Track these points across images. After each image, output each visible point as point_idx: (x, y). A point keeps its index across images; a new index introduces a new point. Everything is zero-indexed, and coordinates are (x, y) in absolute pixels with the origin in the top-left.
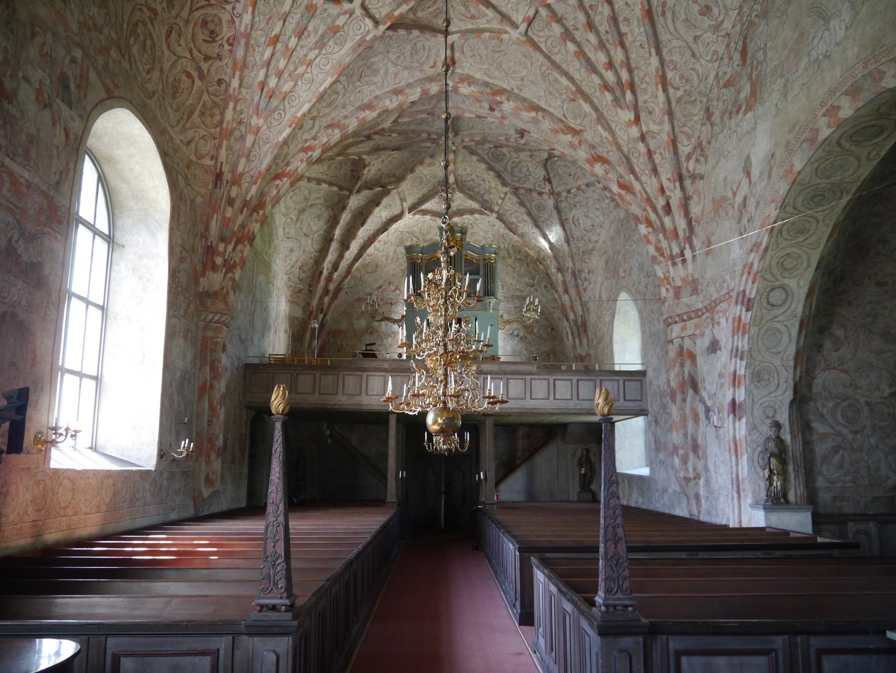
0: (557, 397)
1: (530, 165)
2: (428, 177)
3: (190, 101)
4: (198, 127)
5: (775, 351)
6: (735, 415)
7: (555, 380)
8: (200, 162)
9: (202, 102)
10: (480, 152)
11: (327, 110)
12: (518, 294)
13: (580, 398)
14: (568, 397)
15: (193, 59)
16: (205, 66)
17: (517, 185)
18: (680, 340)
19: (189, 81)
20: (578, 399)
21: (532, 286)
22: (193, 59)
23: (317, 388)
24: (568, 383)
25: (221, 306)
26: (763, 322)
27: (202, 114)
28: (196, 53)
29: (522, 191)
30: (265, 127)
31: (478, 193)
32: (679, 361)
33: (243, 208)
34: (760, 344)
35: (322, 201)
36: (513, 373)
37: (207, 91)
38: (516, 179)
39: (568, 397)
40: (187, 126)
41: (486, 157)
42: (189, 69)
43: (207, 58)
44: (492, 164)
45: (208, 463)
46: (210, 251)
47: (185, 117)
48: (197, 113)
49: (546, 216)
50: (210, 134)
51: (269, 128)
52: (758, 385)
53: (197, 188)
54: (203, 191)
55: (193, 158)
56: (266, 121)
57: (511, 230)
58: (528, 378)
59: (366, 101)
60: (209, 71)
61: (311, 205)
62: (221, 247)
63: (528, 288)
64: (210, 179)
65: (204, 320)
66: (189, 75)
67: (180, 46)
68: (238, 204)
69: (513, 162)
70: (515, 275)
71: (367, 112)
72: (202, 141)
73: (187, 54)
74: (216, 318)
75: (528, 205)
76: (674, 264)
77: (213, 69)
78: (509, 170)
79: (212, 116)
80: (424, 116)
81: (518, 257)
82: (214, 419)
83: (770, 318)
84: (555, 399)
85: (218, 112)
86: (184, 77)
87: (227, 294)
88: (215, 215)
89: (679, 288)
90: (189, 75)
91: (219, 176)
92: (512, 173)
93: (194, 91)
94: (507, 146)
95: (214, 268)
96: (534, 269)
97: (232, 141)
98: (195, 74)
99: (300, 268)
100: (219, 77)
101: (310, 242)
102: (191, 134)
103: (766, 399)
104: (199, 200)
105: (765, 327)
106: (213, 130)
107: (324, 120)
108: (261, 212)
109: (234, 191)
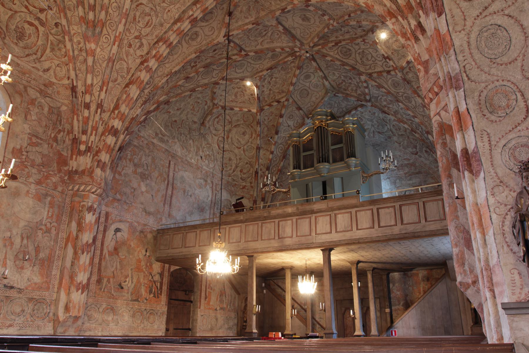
0: (381, 225)
1: (371, 50)
2: (311, 88)
3: (40, 43)
4: (52, 59)
5: (505, 59)
6: (471, 172)
7: (378, 209)
8: (60, 82)
9: (49, 42)
10: (331, 54)
11: (148, 30)
12: (406, 162)
13: (405, 222)
14: (393, 223)
15: (31, 13)
16: (42, 16)
17: (370, 71)
18: (437, 117)
19: (32, 29)
20: (402, 223)
21: (416, 154)
22: (31, 13)
23: (197, 242)
24: (392, 210)
25: (86, 179)
26: (469, 23)
27: (53, 50)
28: (31, 8)
29: (375, 75)
30: (98, 50)
31: (352, 90)
32: (440, 141)
33: (97, 109)
34: (477, 56)
35: (242, 122)
36: (339, 208)
37: (50, 33)
38: (368, 67)
39: (393, 223)
40: (43, 58)
41: (337, 56)
42: (28, 19)
43: (42, 10)
44: (344, 60)
45: (68, 294)
46: (75, 141)
47: (39, 54)
48: (48, 50)
49: (402, 90)
50: (62, 62)
51: (102, 50)
52: (493, 118)
53: (61, 100)
54: (66, 102)
55: (54, 80)
56: (97, 44)
57: (384, 112)
58: (353, 210)
59: (176, 17)
60: (46, 19)
61: (235, 126)
62: (84, 138)
63: (414, 156)
64: (69, 92)
65: (72, 190)
66: (31, 24)
67: (15, 4)
68: (93, 107)
69: (359, 54)
70: (401, 148)
71: (179, 24)
72: (58, 68)
73: (26, 10)
74: (82, 188)
75: (386, 86)
76: (417, 39)
77: (49, 17)
78: (360, 61)
79: (60, 49)
80: (250, 26)
81: (400, 133)
82: (76, 261)
83: (477, 12)
84: (379, 227)
85: (63, 46)
86: (26, 26)
87: (93, 172)
88: (75, 117)
89: (427, 62)
90: (31, 24)
91: (73, 89)
92: (363, 63)
93: (41, 35)
94: (344, 40)
95: (80, 153)
96: (413, 139)
97: (79, 64)
98: (36, 23)
99: (241, 171)
100: (55, 22)
101: (242, 152)
102: (46, 65)
103: (511, 136)
104: (64, 108)
105: (476, 29)
106: (63, 60)
107: (150, 38)
108: (116, 112)
109: (88, 98)
